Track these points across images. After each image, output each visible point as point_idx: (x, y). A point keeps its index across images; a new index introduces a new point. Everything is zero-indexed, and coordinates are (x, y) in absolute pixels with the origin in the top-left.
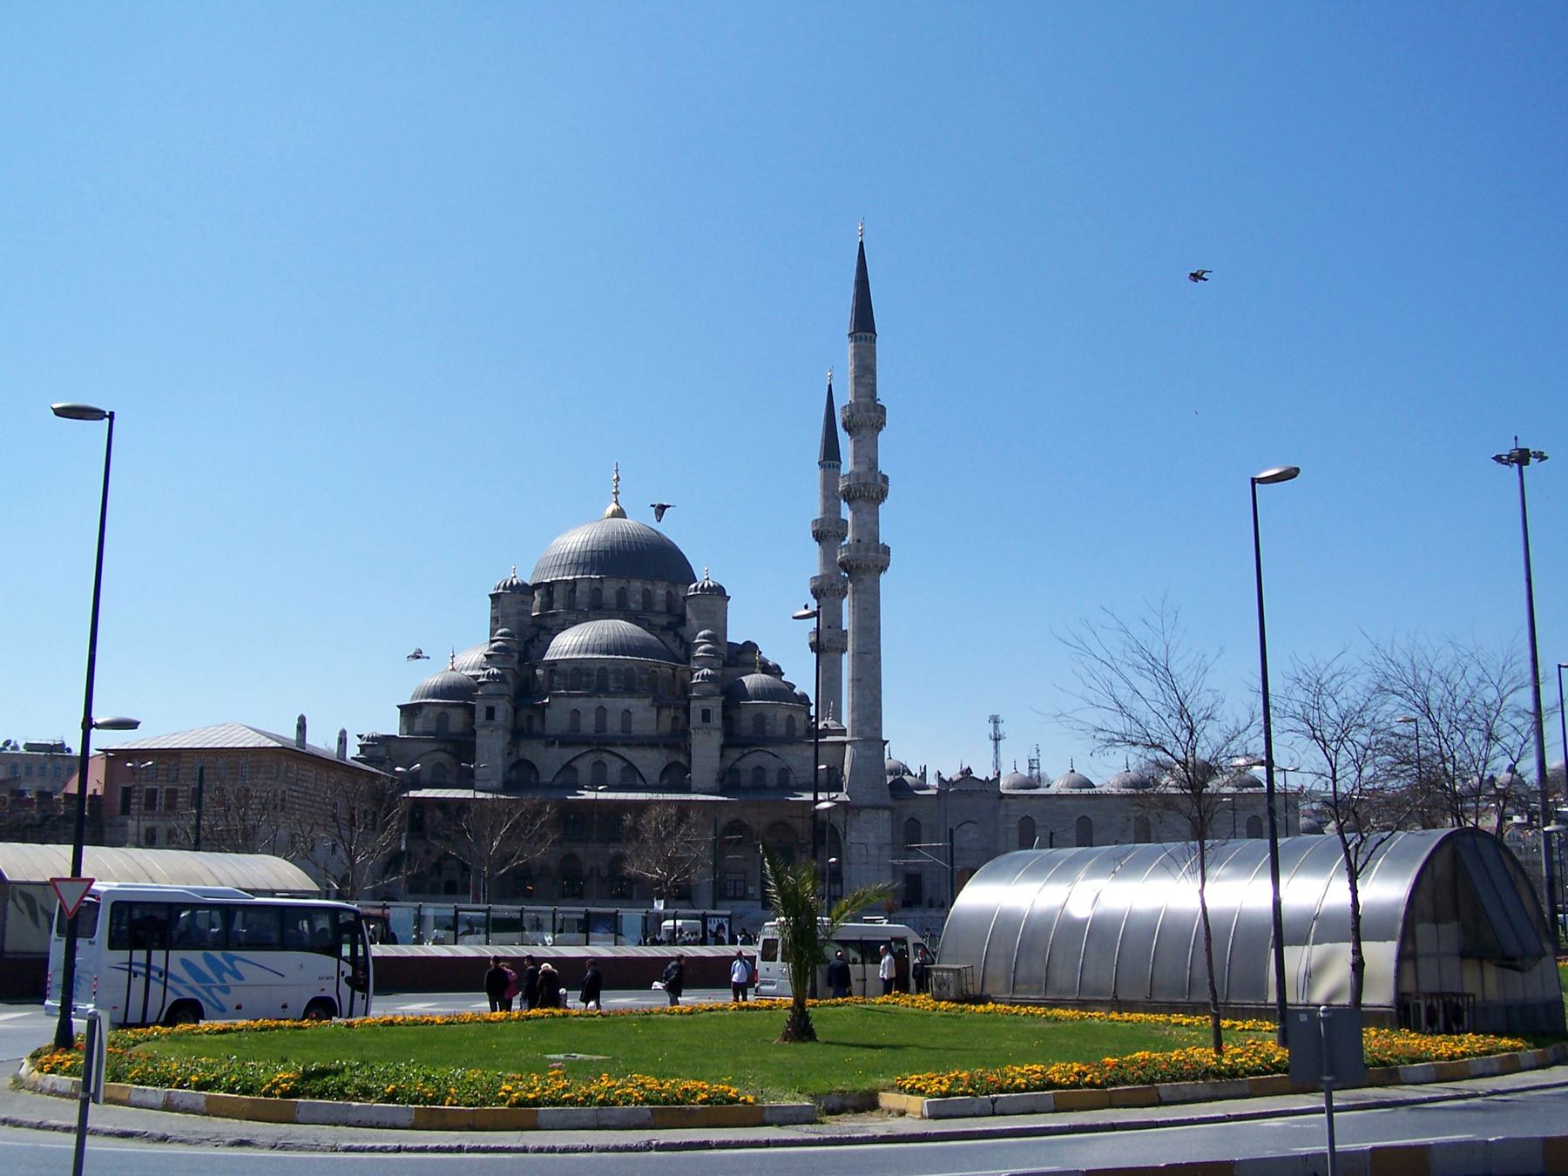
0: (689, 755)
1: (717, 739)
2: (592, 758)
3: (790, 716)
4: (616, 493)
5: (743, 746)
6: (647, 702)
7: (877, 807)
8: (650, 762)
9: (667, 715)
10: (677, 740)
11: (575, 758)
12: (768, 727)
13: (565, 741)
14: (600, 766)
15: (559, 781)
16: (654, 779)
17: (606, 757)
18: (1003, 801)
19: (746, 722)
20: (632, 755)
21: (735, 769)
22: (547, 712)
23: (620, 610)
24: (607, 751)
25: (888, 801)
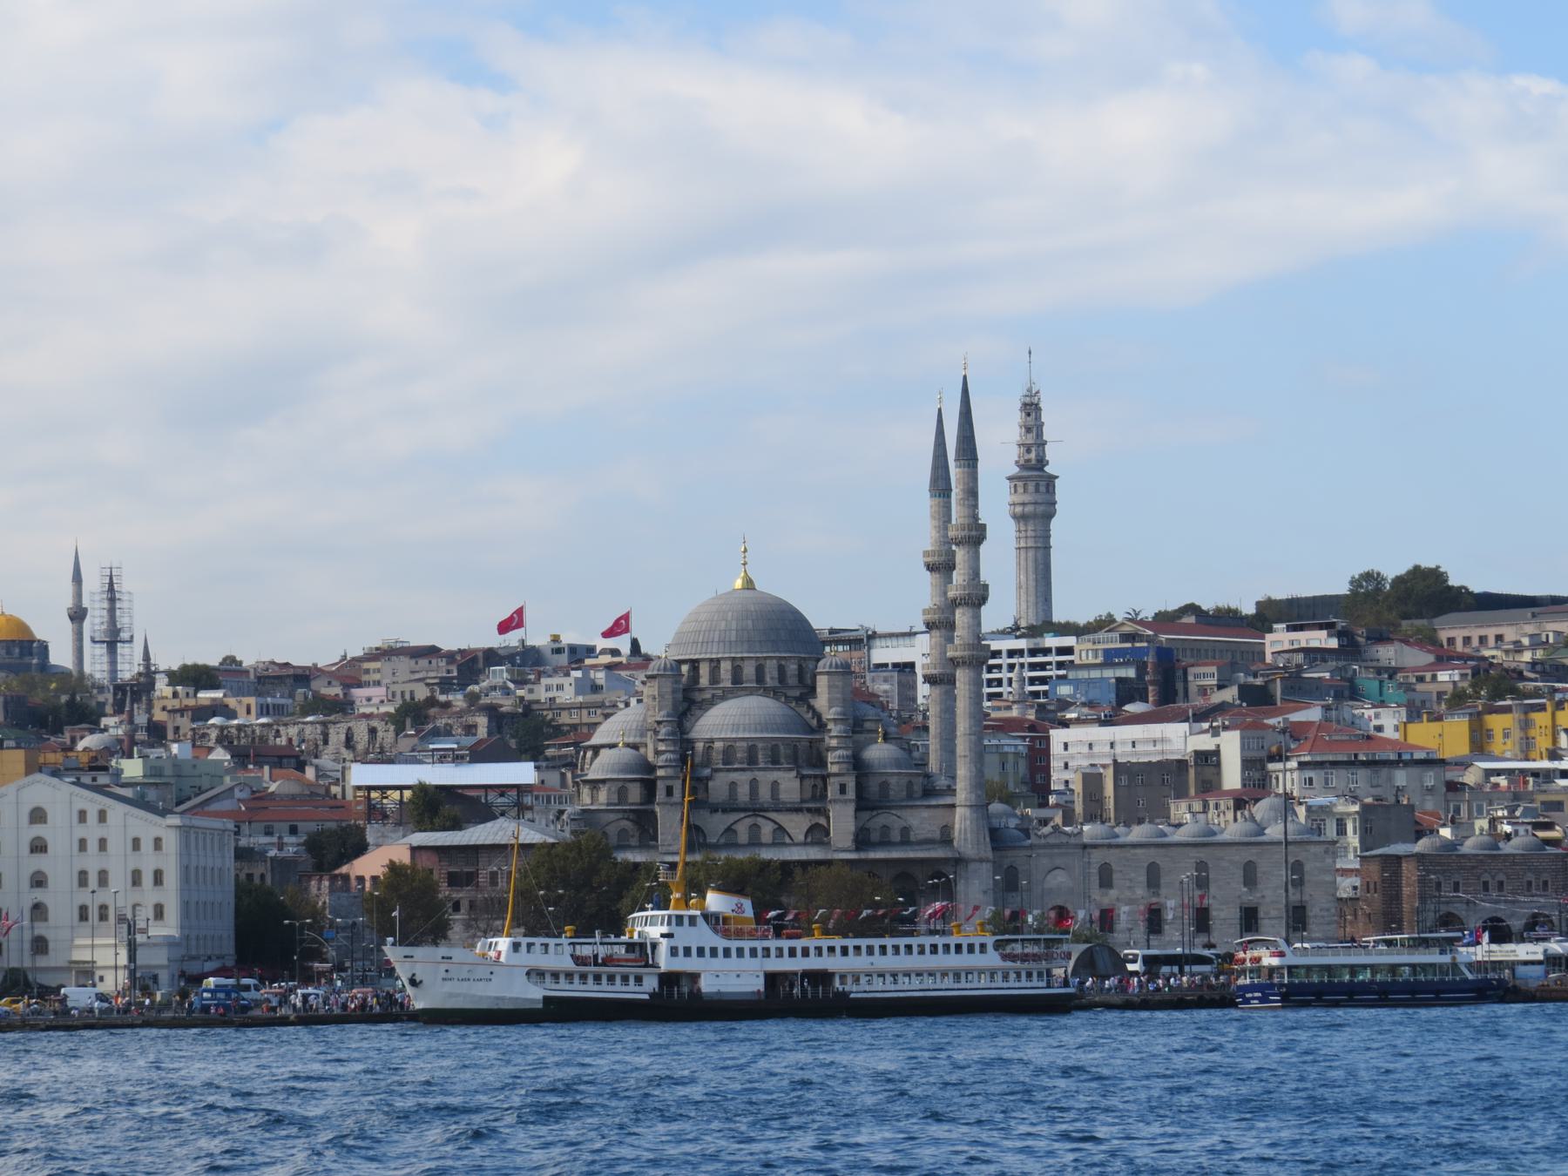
0: (828, 818)
1: (851, 808)
2: (749, 821)
3: (910, 782)
4: (745, 564)
5: (873, 809)
6: (794, 773)
7: (981, 861)
8: (797, 825)
9: (808, 783)
10: (815, 803)
11: (735, 822)
12: (892, 793)
14: (755, 828)
15: (722, 841)
16: (801, 838)
17: (759, 819)
18: (1088, 850)
19: (873, 786)
20: (781, 818)
21: (868, 830)
22: (711, 784)
24: (764, 817)
25: (990, 855)
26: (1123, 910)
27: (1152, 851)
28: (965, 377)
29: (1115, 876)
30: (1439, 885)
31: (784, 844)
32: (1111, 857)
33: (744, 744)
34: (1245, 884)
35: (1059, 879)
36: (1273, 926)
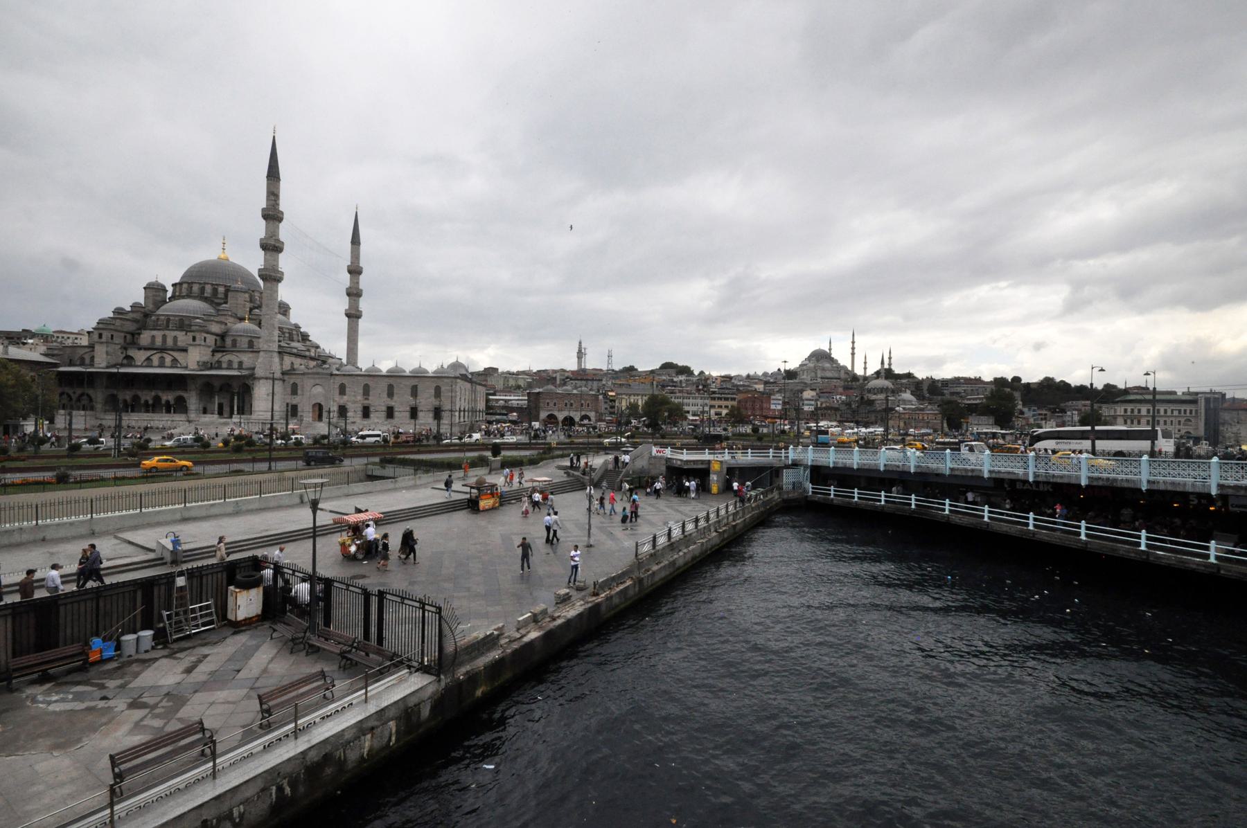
2: (159, 355)
5: (223, 351)
13: (146, 349)
14: (162, 358)
15: (144, 364)
17: (165, 355)
20: (176, 354)
21: (221, 362)
22: (142, 336)
23: (201, 297)
26: (350, 406)
27: (367, 378)
28: (274, 137)
29: (347, 389)
30: (548, 403)
31: (177, 367)
32: (345, 381)
33: (163, 317)
34: (412, 396)
35: (319, 389)
36: (377, 417)
